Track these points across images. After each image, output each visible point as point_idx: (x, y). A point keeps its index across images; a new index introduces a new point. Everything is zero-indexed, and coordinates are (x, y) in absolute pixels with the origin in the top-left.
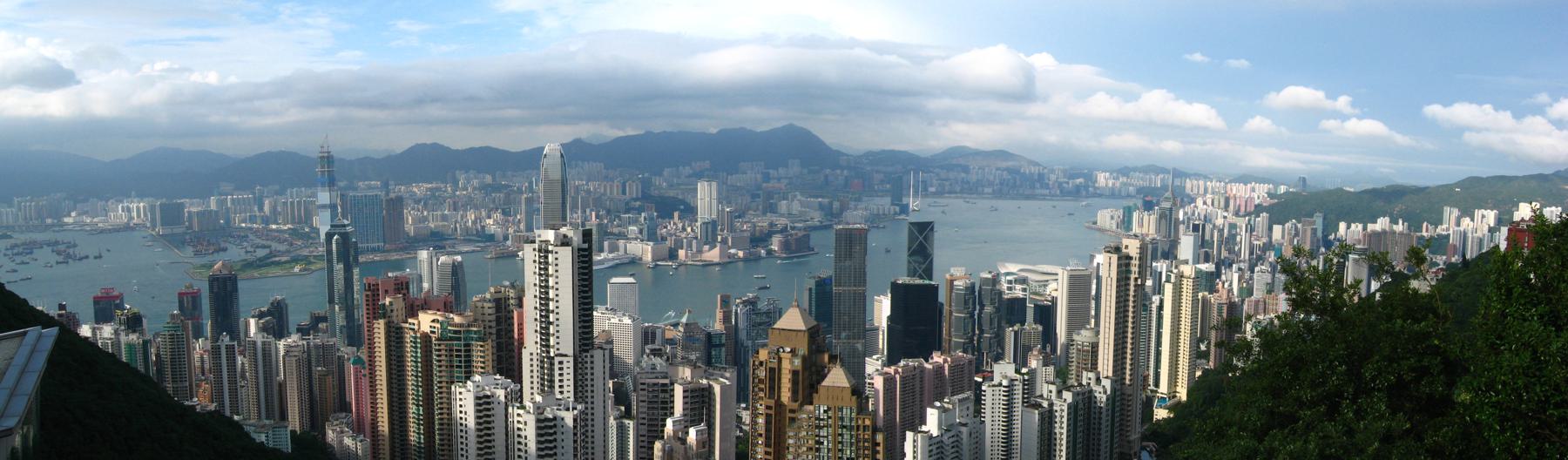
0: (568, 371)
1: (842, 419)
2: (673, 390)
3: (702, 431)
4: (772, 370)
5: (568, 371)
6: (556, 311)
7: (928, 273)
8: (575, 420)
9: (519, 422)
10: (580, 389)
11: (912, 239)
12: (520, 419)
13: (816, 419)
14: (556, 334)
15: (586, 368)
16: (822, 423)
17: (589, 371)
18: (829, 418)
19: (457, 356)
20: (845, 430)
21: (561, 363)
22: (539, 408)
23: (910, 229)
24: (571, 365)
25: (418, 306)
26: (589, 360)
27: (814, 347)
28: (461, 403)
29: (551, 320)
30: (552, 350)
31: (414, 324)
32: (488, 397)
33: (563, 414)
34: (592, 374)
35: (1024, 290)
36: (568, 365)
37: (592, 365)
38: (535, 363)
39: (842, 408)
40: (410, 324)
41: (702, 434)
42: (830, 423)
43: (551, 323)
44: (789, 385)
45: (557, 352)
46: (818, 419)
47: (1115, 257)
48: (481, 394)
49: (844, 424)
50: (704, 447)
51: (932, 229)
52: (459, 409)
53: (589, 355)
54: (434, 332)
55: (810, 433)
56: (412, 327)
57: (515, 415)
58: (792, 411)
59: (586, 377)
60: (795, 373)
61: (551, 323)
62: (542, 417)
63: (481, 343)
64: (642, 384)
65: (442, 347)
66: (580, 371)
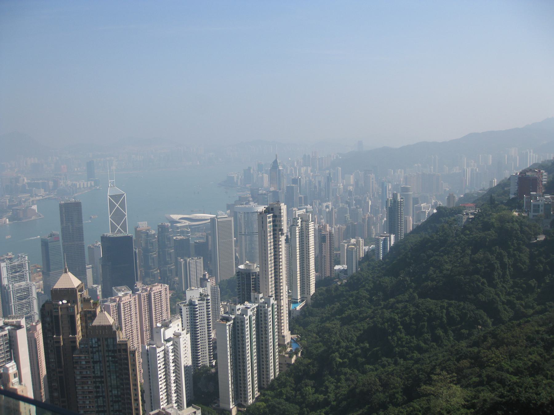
3: (12, 366)
7: (124, 227)
11: (112, 206)
16: (94, 350)
18: (99, 346)
41: (13, 369)
42: (100, 349)
46: (91, 347)
49: (109, 349)
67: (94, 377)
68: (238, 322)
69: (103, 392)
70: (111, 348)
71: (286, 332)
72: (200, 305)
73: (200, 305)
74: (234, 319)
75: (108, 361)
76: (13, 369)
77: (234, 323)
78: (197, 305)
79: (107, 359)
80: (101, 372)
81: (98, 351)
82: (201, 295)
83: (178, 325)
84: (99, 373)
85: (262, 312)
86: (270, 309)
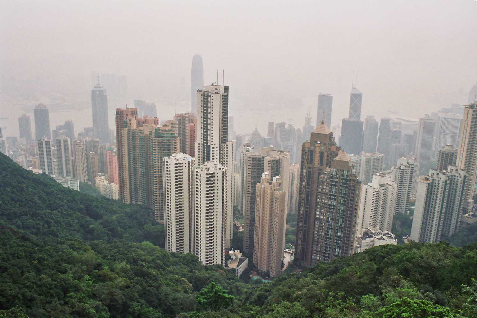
0: (217, 152)
1: (343, 175)
2: (264, 161)
3: (279, 178)
4: (312, 152)
5: (217, 152)
6: (211, 124)
7: (359, 116)
8: (223, 174)
9: (197, 175)
10: (221, 160)
12: (197, 174)
13: (331, 174)
14: (211, 135)
15: (224, 151)
17: (226, 152)
19: (163, 145)
20: (344, 181)
21: (213, 148)
22: (206, 168)
23: (351, 96)
24: (218, 149)
25: (142, 122)
26: (225, 147)
27: (330, 142)
28: (167, 167)
29: (209, 128)
30: (209, 142)
31: (141, 130)
32: (180, 164)
33: (218, 171)
34: (227, 153)
35: (400, 128)
36: (217, 149)
37: (227, 149)
38: (201, 148)
39: (344, 171)
40: (139, 130)
43: (210, 130)
44: (319, 159)
45: (211, 143)
47: (471, 111)
48: (177, 163)
50: (279, 186)
51: (361, 98)
52: (166, 169)
53: (226, 144)
54: (151, 134)
55: (328, 181)
56: (140, 131)
57: (195, 172)
58: (320, 170)
59: (224, 155)
60: (322, 154)
61: (210, 130)
62: (208, 173)
63: (175, 139)
64: (249, 158)
65: (156, 141)
66: (221, 152)
67: (330, 195)
68: (436, 183)
69: (334, 206)
70: (345, 178)
71: (471, 200)
72: (406, 170)
73: (406, 170)
74: (433, 180)
75: (341, 186)
76: (279, 180)
77: (432, 183)
78: (404, 170)
79: (341, 184)
80: (336, 192)
81: (336, 178)
82: (408, 163)
83: (390, 178)
84: (334, 193)
85: (455, 180)
86: (462, 178)
